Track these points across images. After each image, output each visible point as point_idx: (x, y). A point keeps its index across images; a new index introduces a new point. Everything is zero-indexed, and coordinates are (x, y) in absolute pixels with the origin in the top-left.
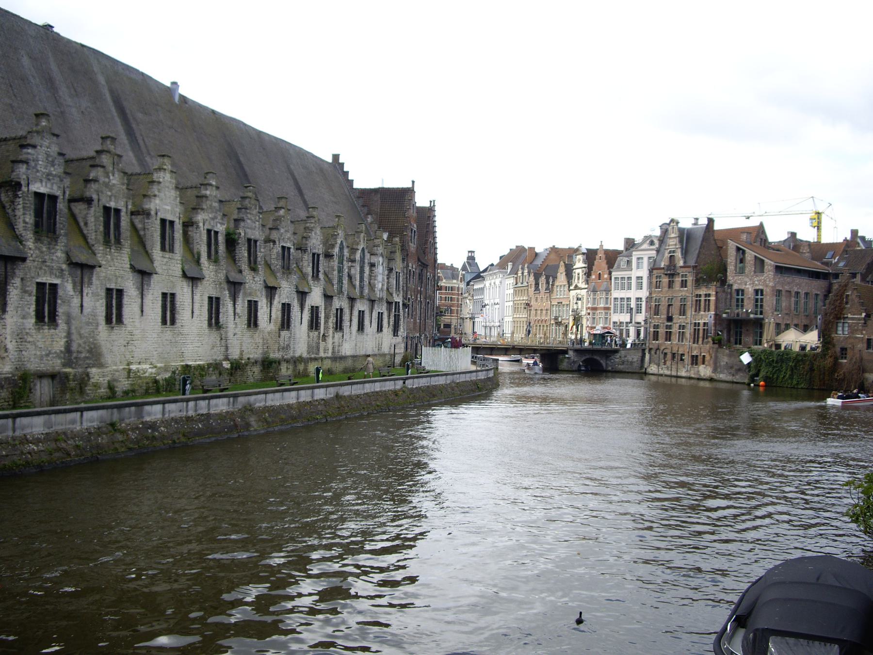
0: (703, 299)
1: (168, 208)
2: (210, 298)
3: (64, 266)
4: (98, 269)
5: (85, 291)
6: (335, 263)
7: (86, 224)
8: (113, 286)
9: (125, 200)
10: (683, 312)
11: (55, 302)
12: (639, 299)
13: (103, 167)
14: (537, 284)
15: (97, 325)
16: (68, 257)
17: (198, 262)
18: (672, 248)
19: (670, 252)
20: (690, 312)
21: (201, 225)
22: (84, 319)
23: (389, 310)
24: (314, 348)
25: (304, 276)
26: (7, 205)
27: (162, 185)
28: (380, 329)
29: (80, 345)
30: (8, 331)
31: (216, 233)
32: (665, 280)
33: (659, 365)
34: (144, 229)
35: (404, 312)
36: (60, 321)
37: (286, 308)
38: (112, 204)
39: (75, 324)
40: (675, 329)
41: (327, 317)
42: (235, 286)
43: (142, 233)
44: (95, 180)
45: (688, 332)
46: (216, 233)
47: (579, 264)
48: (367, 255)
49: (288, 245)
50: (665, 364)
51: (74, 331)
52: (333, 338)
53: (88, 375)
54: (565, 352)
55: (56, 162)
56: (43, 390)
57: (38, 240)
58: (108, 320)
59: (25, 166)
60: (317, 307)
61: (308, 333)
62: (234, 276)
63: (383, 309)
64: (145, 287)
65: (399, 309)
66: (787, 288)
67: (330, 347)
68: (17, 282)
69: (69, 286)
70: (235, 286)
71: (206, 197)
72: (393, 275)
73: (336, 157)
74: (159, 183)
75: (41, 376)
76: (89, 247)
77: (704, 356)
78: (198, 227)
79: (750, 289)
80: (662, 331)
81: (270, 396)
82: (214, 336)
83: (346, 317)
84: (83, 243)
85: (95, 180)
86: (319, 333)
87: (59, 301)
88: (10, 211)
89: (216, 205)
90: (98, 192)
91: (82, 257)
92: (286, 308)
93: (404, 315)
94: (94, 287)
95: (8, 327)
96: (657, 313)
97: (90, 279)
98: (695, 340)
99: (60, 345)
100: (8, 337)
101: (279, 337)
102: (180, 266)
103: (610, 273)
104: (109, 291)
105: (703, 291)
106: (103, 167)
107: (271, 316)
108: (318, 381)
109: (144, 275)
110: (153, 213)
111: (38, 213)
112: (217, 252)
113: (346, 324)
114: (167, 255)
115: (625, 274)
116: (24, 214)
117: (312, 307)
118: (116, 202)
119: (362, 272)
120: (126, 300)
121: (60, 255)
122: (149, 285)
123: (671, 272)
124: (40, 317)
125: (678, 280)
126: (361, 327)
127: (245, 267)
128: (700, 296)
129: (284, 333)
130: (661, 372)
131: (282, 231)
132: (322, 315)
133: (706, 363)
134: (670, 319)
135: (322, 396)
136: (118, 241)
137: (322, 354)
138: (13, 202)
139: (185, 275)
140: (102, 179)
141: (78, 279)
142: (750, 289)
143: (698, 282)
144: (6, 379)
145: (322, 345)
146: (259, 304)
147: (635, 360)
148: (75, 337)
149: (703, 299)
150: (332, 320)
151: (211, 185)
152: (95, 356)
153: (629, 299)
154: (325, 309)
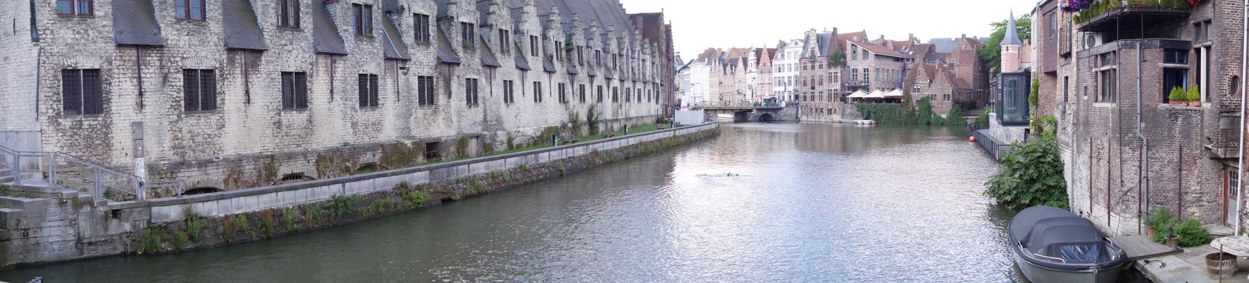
1: (534, 28)
2: (559, 84)
3: (480, 68)
4: (499, 68)
5: (493, 82)
7: (489, 41)
11: (476, 90)
13: (497, 4)
15: (500, 104)
16: (482, 62)
17: (551, 62)
21: (552, 38)
22: (493, 100)
24: (616, 113)
25: (607, 68)
26: (445, 32)
27: (529, 15)
29: (491, 117)
31: (560, 43)
34: (521, 42)
36: (479, 102)
37: (600, 88)
39: (488, 104)
41: (622, 94)
42: (572, 75)
43: (519, 45)
44: (494, 13)
46: (560, 43)
49: (599, 49)
51: (487, 108)
53: (496, 134)
55: (472, 3)
56: (473, 146)
57: (465, 52)
58: (506, 101)
59: (455, 6)
62: (571, 70)
64: (524, 79)
67: (624, 112)
68: (455, 78)
70: (572, 75)
71: (553, 20)
74: (528, 13)
76: (492, 55)
78: (550, 40)
81: (606, 143)
82: (563, 106)
84: (489, 53)
85: (494, 13)
87: (478, 90)
88: (447, 35)
89: (559, 25)
90: (496, 21)
91: (490, 62)
92: (600, 88)
94: (497, 80)
97: (495, 75)
99: (480, 117)
100: (453, 114)
102: (542, 65)
104: (505, 81)
106: (497, 4)
108: (626, 134)
109: (523, 70)
110: (526, 32)
111: (464, 36)
112: (561, 55)
114: (535, 58)
116: (457, 36)
120: (514, 87)
121: (477, 60)
122: (526, 77)
124: (469, 100)
127: (577, 64)
131: (595, 40)
132: (619, 92)
135: (633, 143)
136: (508, 51)
137: (620, 117)
138: (449, 29)
139: (545, 70)
140: (497, 12)
141: (488, 76)
144: (453, 140)
145: (620, 110)
146: (586, 87)
148: (488, 111)
150: (624, 95)
151: (555, 13)
152: (499, 121)
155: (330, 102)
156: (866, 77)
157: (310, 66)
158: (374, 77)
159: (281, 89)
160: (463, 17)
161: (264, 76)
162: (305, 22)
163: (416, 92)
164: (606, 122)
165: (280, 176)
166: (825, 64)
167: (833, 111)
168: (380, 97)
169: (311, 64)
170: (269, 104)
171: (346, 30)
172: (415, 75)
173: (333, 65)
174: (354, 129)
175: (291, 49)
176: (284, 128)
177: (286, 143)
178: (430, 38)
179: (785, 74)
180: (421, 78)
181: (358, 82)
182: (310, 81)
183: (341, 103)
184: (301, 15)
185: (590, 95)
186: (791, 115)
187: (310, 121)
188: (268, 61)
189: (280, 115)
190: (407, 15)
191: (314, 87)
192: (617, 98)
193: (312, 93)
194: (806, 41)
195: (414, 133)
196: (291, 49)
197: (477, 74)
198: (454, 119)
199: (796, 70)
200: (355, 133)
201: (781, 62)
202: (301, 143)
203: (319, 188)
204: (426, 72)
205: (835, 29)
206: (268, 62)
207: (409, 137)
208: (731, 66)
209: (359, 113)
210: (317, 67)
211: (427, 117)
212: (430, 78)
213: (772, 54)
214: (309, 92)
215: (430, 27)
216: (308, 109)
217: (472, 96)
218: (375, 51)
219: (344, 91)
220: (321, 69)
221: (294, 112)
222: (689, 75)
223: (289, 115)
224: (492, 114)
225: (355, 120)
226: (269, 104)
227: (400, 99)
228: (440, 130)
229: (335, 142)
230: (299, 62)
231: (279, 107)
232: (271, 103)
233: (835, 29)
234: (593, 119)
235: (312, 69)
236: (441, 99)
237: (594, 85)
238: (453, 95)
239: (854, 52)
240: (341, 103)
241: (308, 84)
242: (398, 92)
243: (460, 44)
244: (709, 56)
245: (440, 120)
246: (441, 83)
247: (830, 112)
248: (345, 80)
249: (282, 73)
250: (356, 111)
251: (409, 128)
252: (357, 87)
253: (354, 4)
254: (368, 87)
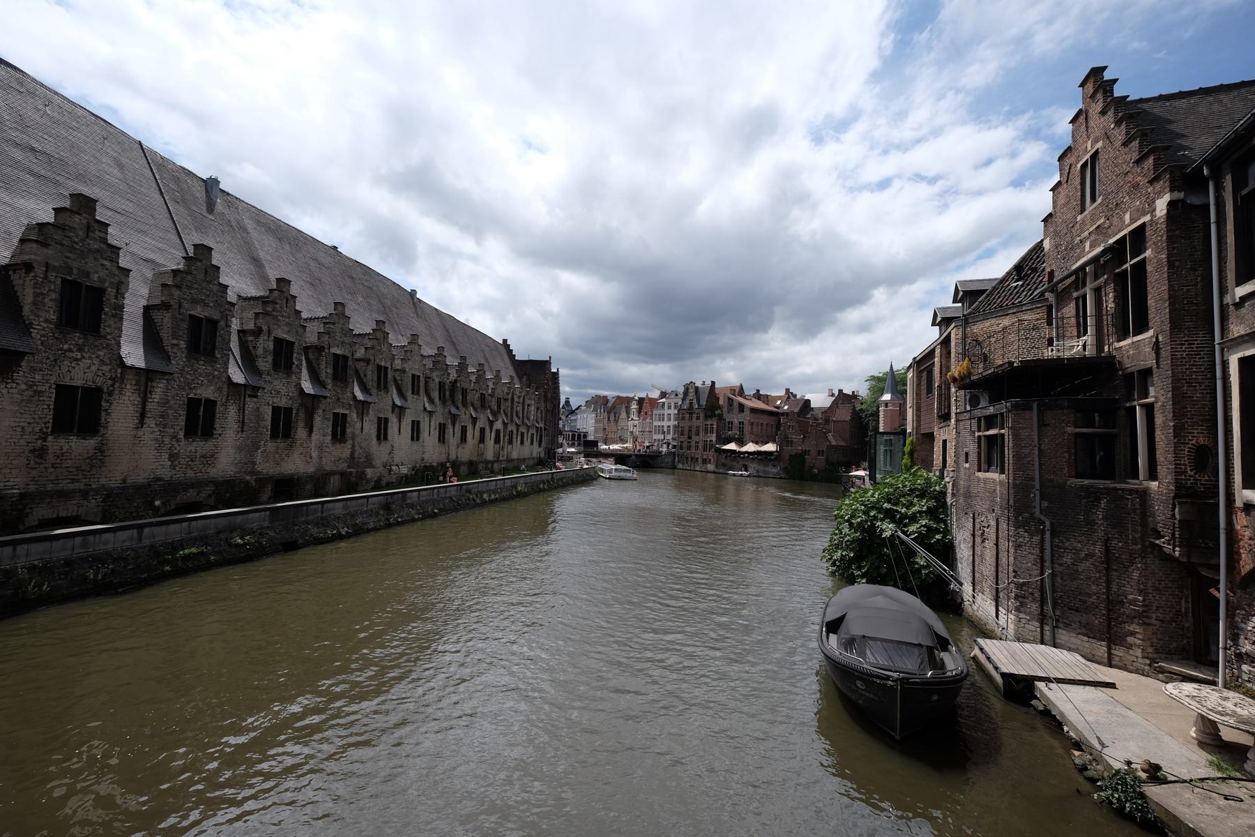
2: (440, 424)
3: (351, 403)
6: (509, 403)
7: (365, 375)
8: (382, 416)
10: (698, 434)
12: (669, 427)
14: (609, 419)
18: (691, 398)
20: (702, 434)
23: (537, 432)
24: (497, 455)
28: (532, 443)
30: (313, 444)
32: (687, 416)
37: (482, 430)
38: (383, 364)
39: (358, 440)
40: (693, 444)
41: (504, 436)
45: (701, 445)
47: (634, 406)
48: (526, 400)
51: (356, 444)
52: (508, 448)
53: (364, 472)
54: (630, 456)
56: (335, 481)
58: (378, 438)
63: (534, 432)
66: (757, 421)
68: (320, 412)
69: (355, 416)
70: (454, 418)
72: (539, 412)
73: (505, 341)
75: (333, 473)
79: (736, 421)
80: (685, 445)
83: (515, 436)
90: (374, 355)
92: (482, 430)
94: (370, 416)
95: (313, 442)
96: (682, 434)
98: (705, 450)
99: (347, 453)
103: (652, 412)
104: (379, 419)
105: (709, 423)
111: (335, 367)
113: (514, 440)
115: (661, 412)
118: (386, 362)
119: (523, 409)
120: (390, 425)
122: (404, 415)
123: (690, 410)
124: (334, 436)
125: (695, 416)
126: (522, 442)
127: (460, 405)
129: (481, 445)
134: (690, 438)
136: (386, 387)
141: (360, 411)
142: (736, 421)
143: (706, 417)
145: (501, 452)
150: (507, 437)
152: (369, 462)
153: (663, 426)
155: (137, 428)
156: (741, 429)
157: (110, 382)
158: (211, 404)
159: (52, 407)
160: (336, 348)
161: (23, 387)
162: (109, 326)
163: (269, 423)
164: (487, 462)
165: (33, 519)
166: (702, 415)
167: (708, 461)
168: (217, 426)
169: (111, 379)
170: (26, 425)
171: (177, 345)
172: (268, 404)
173: (149, 384)
174: (172, 462)
175: (79, 356)
176: (51, 458)
177: (52, 477)
178: (294, 366)
179: (665, 423)
180: (276, 410)
181: (185, 407)
182: (107, 401)
183: (157, 430)
184: (103, 317)
185: (471, 436)
187: (100, 449)
188: (31, 367)
189: (45, 440)
190: (266, 338)
191: (113, 407)
193: (108, 414)
194: (686, 393)
195: (259, 468)
196: (79, 356)
197: (347, 409)
198: (315, 454)
199: (675, 420)
200: (173, 467)
201: (661, 412)
202: (80, 477)
203: (97, 536)
204: (283, 402)
205: (713, 383)
206: (33, 370)
207: (252, 473)
208: (615, 414)
209: (182, 443)
210: (122, 382)
211: (280, 451)
212: (288, 411)
213: (653, 402)
214: (103, 414)
215: (295, 355)
216: (100, 434)
217: (339, 429)
218: (216, 373)
219: (162, 416)
220: (128, 386)
221: (72, 438)
222: (576, 420)
223: (63, 441)
224: (361, 451)
225: (175, 451)
226: (26, 425)
227: (245, 428)
228: (297, 463)
229: (141, 478)
230: (90, 376)
231: (45, 430)
232: (30, 423)
233: (713, 383)
235: (112, 386)
236: (301, 433)
237: (477, 426)
238: (315, 429)
239: (731, 405)
240: (157, 430)
241: (104, 404)
242: (243, 422)
243: (330, 376)
244: (599, 403)
245: (296, 455)
246: (302, 416)
247: (705, 461)
248: (165, 403)
249: (58, 385)
250: (178, 441)
251: (254, 463)
252: (183, 413)
253: (190, 315)
254: (201, 414)
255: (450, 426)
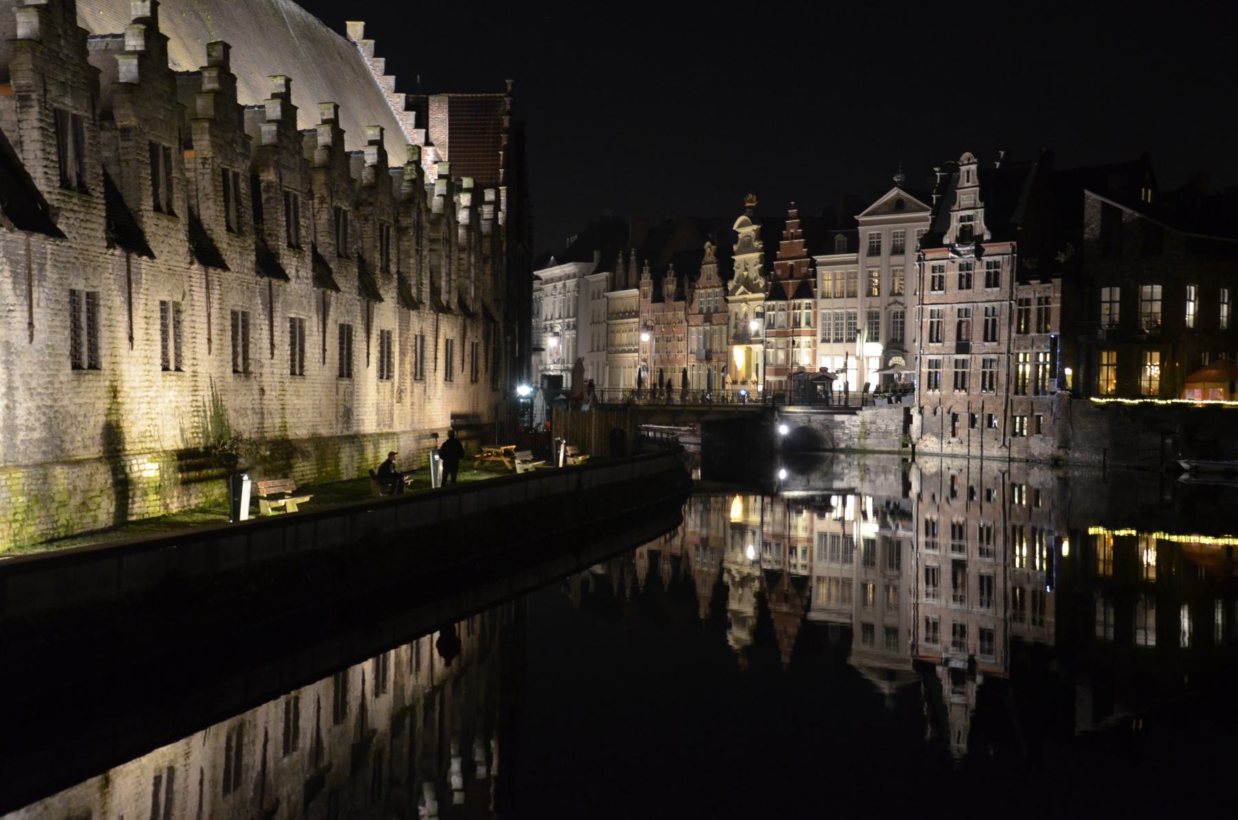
0: (1034, 307)
2: (234, 313)
8: (80, 286)
9: (88, 94)
19: (962, 219)
33: (941, 436)
35: (506, 342)
46: (236, 175)
50: (954, 435)
60: (389, 333)
61: (377, 385)
65: (499, 337)
77: (1039, 417)
83: (429, 353)
86: (393, 384)
92: (346, 334)
93: (506, 347)
101: (337, 393)
107: (324, 350)
113: (429, 365)
117: (382, 331)
122: (139, 283)
128: (1028, 302)
129: (345, 382)
130: (947, 449)
133: (1044, 431)
137: (397, 428)
146: (307, 324)
147: (893, 428)
149: (1034, 307)
154: (401, 335)
186: (886, 433)
192: (390, 364)
234: (677, 398)
237: (330, 322)
255: (259, 321)
